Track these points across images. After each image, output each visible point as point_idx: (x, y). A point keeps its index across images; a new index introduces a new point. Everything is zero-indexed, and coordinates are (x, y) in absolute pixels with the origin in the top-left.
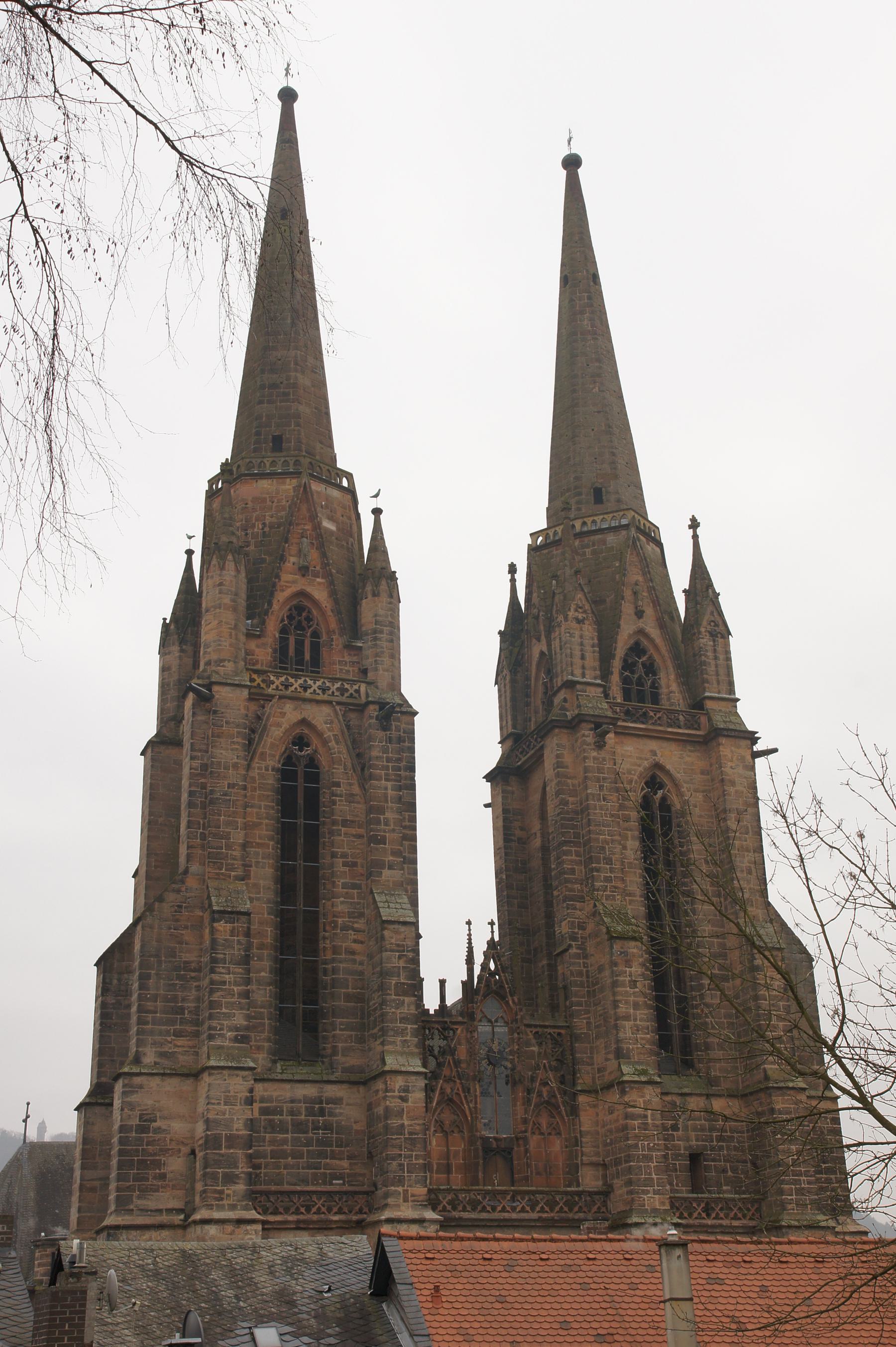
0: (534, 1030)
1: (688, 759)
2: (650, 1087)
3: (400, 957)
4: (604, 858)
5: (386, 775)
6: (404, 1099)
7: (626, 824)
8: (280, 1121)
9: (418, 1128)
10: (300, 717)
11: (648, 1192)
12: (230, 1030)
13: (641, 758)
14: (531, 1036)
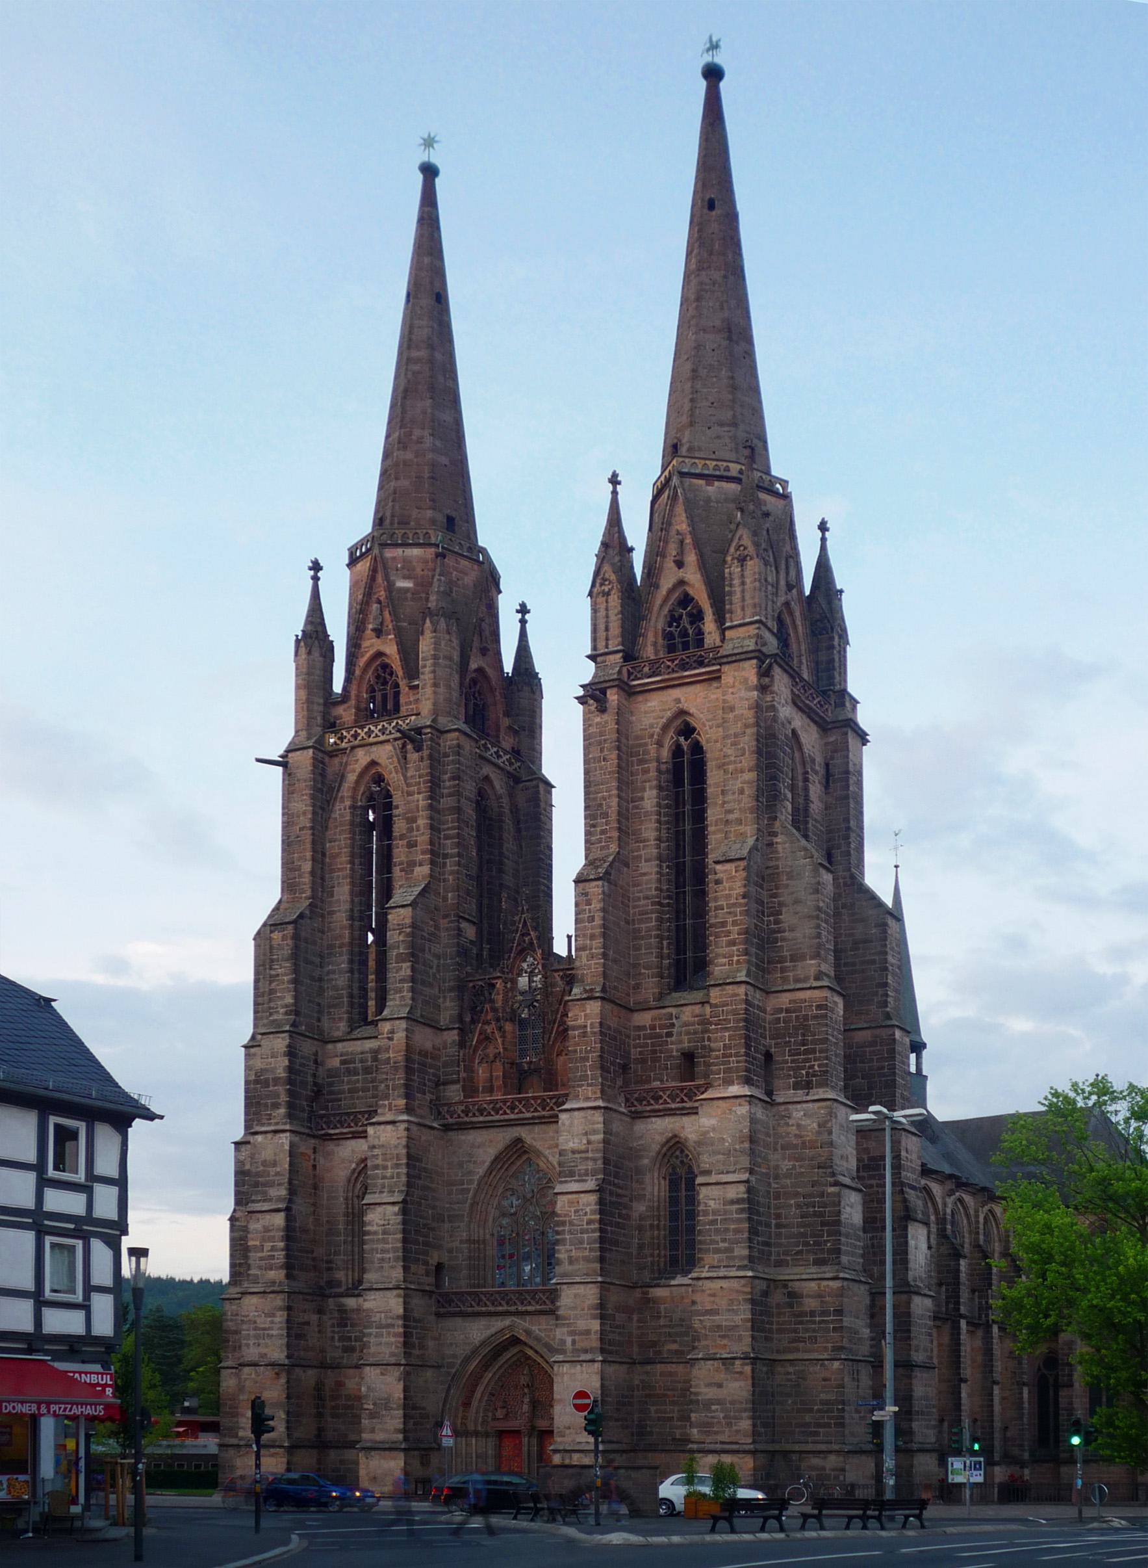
0: (561, 974)
1: (713, 697)
2: (591, 1002)
3: (400, 934)
4: (601, 814)
5: (418, 789)
6: (390, 1039)
7: (645, 777)
8: (354, 1068)
9: (400, 1058)
10: (369, 760)
11: (583, 1085)
12: (283, 1007)
13: (664, 710)
14: (558, 979)
